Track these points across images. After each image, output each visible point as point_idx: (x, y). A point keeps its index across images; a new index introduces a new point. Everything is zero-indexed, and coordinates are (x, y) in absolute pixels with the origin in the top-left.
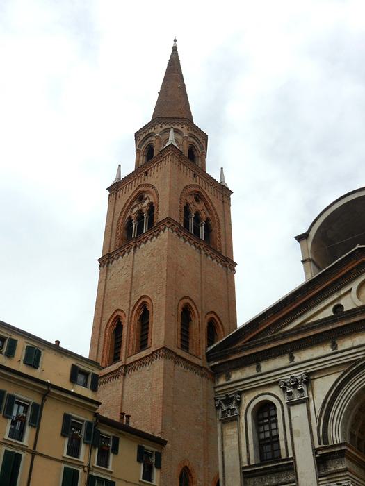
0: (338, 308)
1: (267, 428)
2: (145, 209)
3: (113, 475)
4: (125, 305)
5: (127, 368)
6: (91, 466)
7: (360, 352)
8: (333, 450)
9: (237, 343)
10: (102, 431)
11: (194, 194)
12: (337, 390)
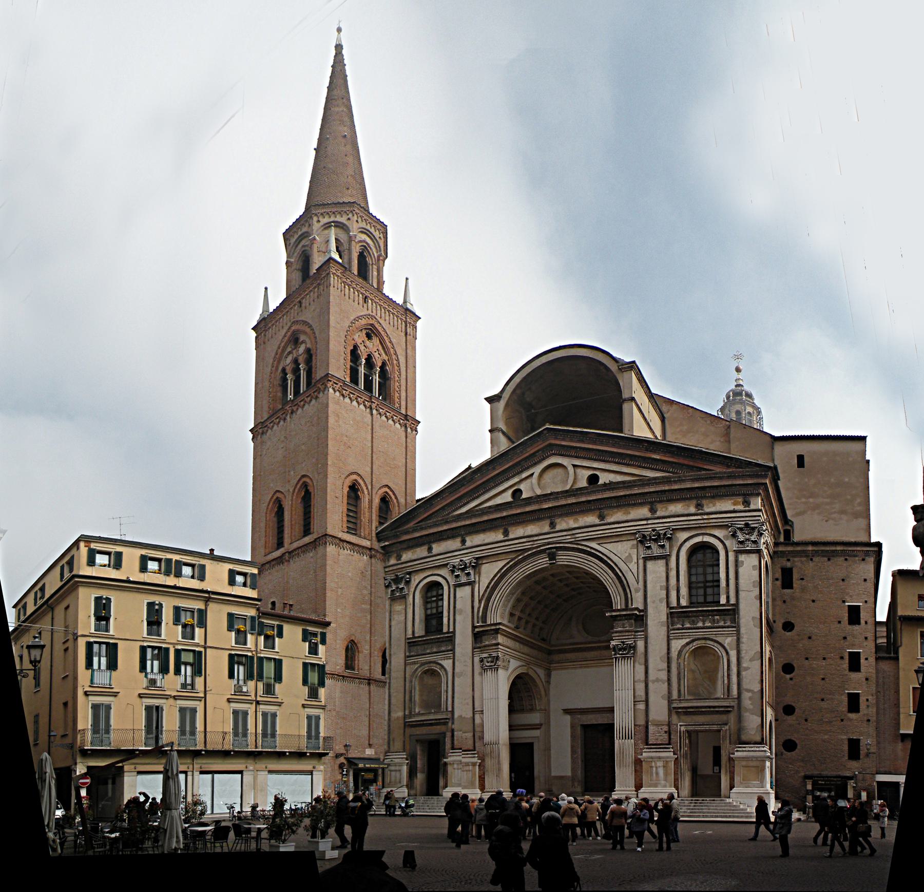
1: (434, 605)
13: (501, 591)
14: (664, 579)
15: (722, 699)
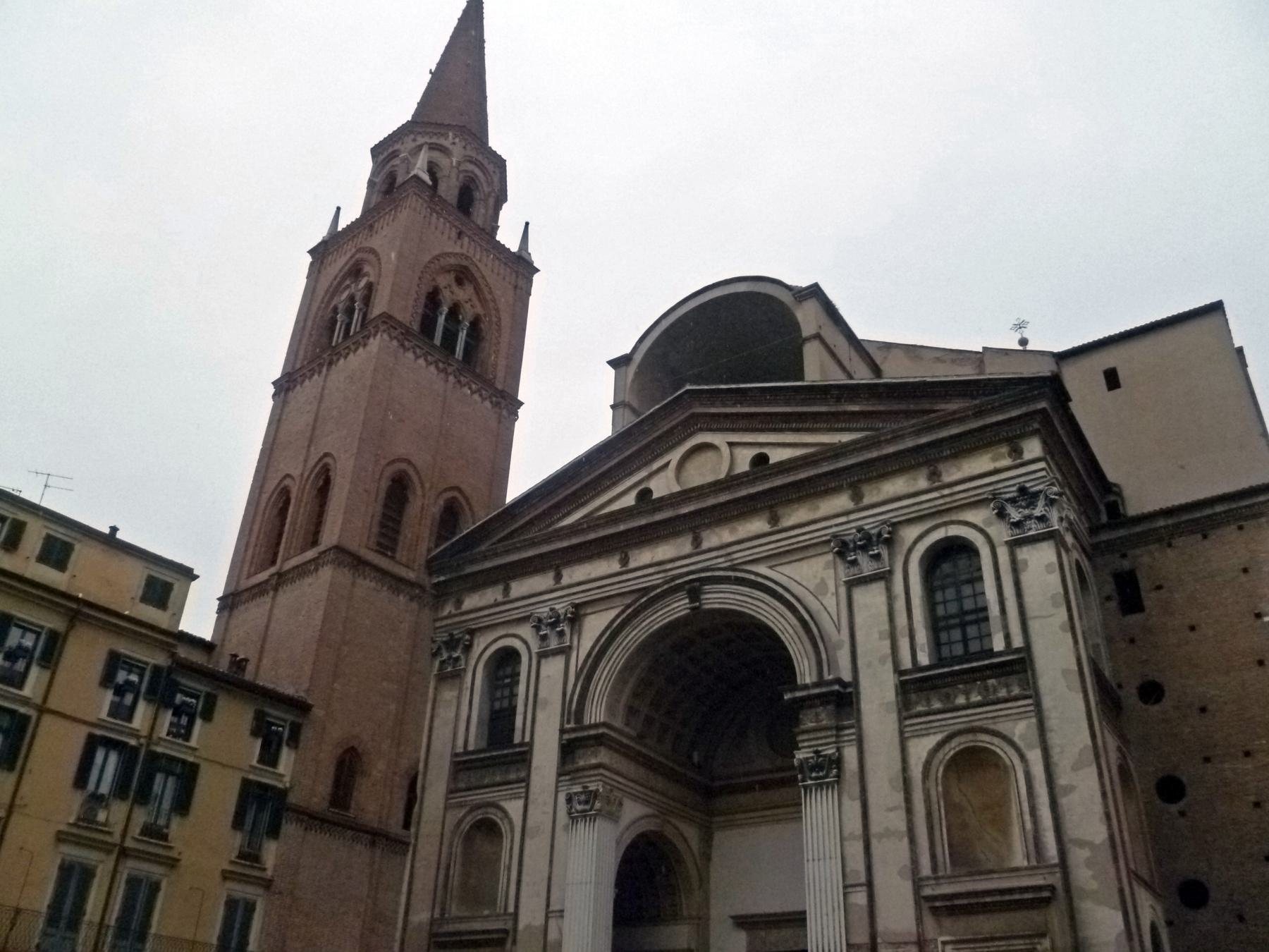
0: (645, 494)
1: (507, 693)
2: (359, 293)
3: (197, 754)
4: (294, 466)
5: (281, 579)
6: (155, 737)
7: (658, 573)
8: (585, 734)
9: (479, 545)
10: (184, 681)
11: (455, 270)
12: (613, 633)
13: (611, 662)
14: (885, 618)
15: (1026, 869)
